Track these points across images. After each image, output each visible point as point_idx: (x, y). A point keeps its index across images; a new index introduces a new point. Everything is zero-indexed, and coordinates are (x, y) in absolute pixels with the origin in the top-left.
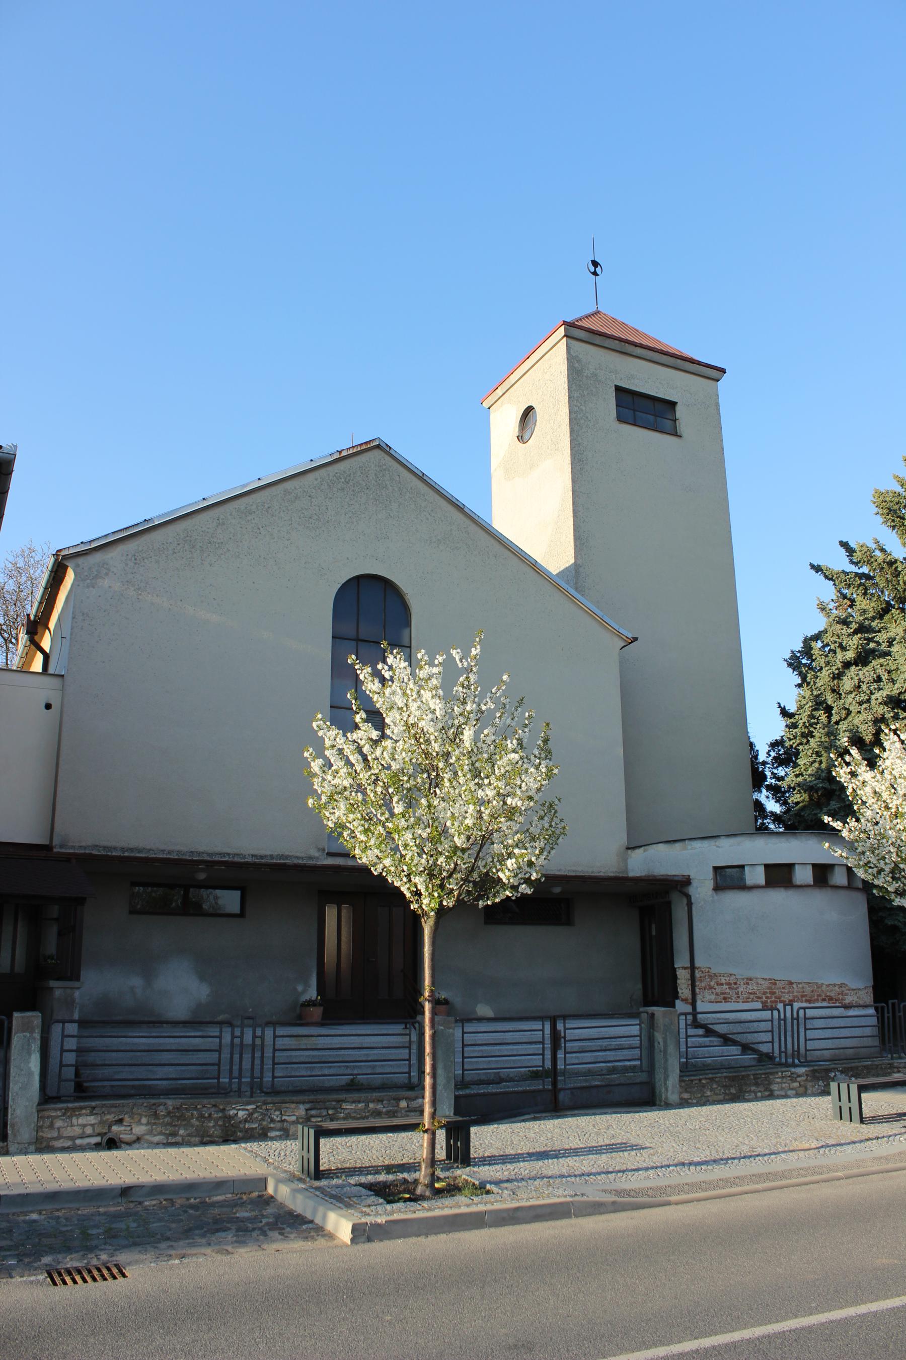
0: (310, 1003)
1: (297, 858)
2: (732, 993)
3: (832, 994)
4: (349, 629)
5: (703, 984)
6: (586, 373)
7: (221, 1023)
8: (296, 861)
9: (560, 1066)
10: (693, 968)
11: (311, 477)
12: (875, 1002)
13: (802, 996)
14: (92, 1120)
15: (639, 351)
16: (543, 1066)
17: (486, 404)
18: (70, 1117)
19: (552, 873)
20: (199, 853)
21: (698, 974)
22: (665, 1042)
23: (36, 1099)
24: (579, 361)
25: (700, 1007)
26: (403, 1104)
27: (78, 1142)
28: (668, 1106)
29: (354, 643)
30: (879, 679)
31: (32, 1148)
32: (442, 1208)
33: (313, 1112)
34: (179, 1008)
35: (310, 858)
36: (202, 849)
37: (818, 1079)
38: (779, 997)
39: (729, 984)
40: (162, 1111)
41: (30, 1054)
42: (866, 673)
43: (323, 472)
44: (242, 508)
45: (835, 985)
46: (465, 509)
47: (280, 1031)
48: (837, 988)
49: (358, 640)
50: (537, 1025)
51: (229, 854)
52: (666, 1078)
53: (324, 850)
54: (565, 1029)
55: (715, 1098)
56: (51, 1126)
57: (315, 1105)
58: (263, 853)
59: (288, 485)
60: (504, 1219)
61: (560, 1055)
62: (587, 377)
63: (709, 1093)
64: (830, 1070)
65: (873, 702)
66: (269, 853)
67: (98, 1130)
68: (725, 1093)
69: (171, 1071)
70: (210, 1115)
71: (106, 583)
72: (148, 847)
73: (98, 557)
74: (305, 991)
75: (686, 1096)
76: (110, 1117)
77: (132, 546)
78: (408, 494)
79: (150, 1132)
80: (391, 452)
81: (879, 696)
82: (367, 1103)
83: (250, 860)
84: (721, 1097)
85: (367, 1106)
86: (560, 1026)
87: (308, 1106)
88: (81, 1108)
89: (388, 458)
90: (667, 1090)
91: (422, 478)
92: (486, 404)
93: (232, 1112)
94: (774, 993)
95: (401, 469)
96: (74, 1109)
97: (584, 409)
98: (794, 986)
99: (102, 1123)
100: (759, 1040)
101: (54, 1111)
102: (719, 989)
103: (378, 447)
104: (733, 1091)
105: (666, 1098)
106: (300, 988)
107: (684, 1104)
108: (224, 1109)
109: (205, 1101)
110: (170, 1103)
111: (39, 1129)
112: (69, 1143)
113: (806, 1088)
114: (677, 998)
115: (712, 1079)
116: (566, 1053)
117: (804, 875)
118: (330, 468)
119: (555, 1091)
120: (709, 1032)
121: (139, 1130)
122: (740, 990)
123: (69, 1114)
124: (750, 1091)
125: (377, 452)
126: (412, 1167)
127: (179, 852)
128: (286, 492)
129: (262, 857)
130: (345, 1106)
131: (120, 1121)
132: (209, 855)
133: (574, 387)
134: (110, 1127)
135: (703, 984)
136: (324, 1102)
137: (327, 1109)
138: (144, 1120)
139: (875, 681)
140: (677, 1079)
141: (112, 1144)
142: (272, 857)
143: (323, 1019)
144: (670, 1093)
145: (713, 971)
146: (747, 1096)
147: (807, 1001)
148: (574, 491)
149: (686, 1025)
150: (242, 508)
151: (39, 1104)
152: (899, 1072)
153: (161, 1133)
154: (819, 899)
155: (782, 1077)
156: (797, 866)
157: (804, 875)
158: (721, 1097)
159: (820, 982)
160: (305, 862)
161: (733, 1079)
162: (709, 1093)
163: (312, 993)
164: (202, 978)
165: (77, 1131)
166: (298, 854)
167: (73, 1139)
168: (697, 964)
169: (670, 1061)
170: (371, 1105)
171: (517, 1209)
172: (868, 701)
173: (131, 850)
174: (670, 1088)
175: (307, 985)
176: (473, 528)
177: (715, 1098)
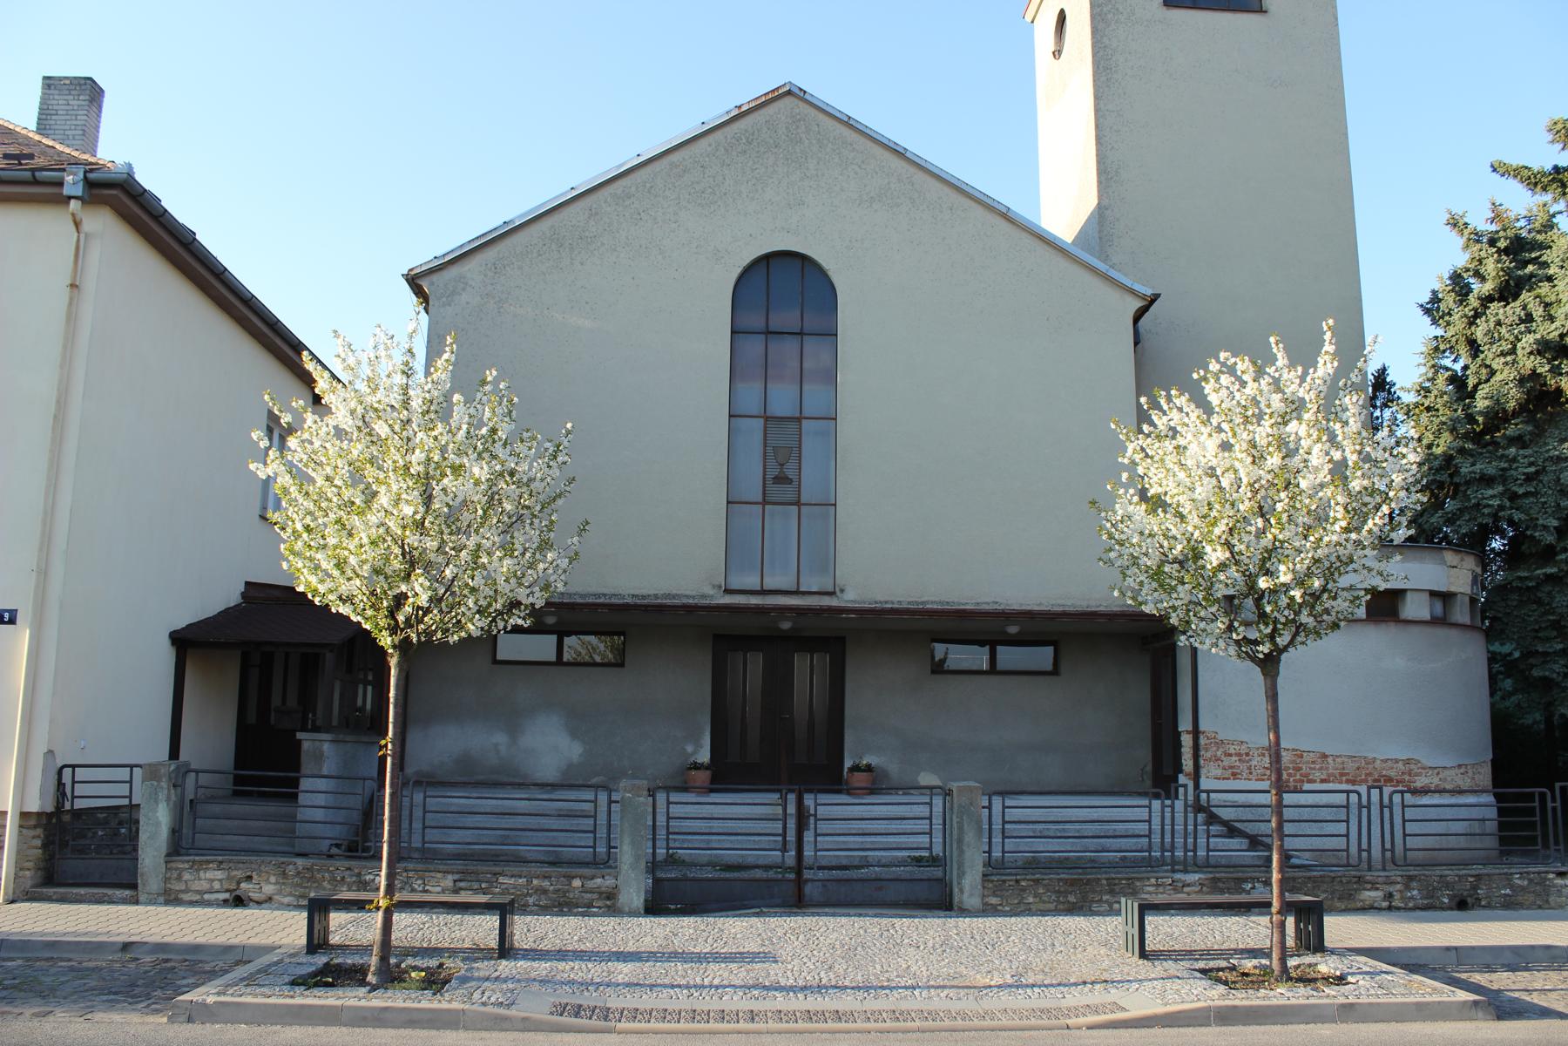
0: (696, 766)
1: (687, 597)
2: (1243, 766)
3: (1392, 774)
4: (757, 321)
5: (1208, 755)
7: (596, 787)
8: (685, 601)
9: (808, 852)
10: (1196, 733)
11: (704, 142)
12: (1495, 786)
13: (1342, 775)
14: (219, 874)
16: (930, 849)
17: (1028, 18)
18: (198, 870)
21: (1203, 741)
22: (961, 829)
23: (164, 850)
25: (1205, 784)
26: (577, 883)
27: (206, 896)
28: (964, 912)
29: (763, 337)
30: (1529, 318)
31: (161, 899)
32: (256, 996)
33: (462, 884)
34: (548, 767)
35: (704, 596)
38: (1306, 775)
39: (1239, 755)
40: (291, 870)
41: (156, 802)
42: (1513, 310)
43: (719, 135)
45: (1397, 761)
47: (674, 797)
48: (1400, 765)
49: (768, 332)
52: (961, 875)
54: (817, 805)
55: (1041, 906)
56: (179, 878)
57: (465, 875)
58: (644, 592)
59: (675, 157)
60: (365, 1019)
61: (808, 836)
63: (1031, 900)
64: (1245, 880)
65: (1519, 352)
66: (652, 592)
67: (226, 886)
68: (1058, 902)
69: (467, 835)
70: (343, 879)
71: (464, 297)
73: (454, 271)
74: (695, 753)
75: (994, 900)
76: (238, 874)
77: (491, 254)
79: (280, 892)
81: (1528, 341)
82: (530, 879)
83: (629, 600)
84: (1052, 906)
85: (530, 882)
86: (809, 800)
87: (456, 877)
88: (208, 862)
90: (961, 891)
91: (848, 123)
92: (1028, 18)
93: (368, 878)
94: (1299, 769)
95: (821, 116)
96: (201, 863)
98: (1330, 760)
99: (229, 878)
101: (181, 864)
102: (1227, 762)
103: (789, 93)
104: (1072, 899)
105: (961, 902)
106: (690, 749)
107: (987, 911)
108: (359, 875)
109: (338, 864)
110: (300, 862)
111: (167, 880)
112: (198, 897)
114: (1181, 771)
115: (1037, 881)
116: (816, 835)
118: (726, 129)
119: (800, 882)
120: (1212, 819)
121: (269, 889)
122: (1254, 763)
123: (197, 867)
124: (1100, 901)
125: (788, 100)
126: (365, 949)
129: (644, 597)
130: (501, 879)
131: (249, 878)
132: (582, 596)
134: (239, 883)
135: (1208, 755)
136: (476, 873)
137: (480, 882)
138: (273, 879)
139: (1522, 321)
140: (979, 878)
141: (239, 901)
142: (656, 596)
143: (712, 782)
144: (966, 895)
145: (1220, 737)
146: (1095, 907)
147: (1348, 781)
148: (1097, 111)
149: (1186, 806)
151: (168, 855)
153: (290, 894)
154: (1377, 640)
155: (1158, 885)
158: (1052, 906)
159: (1371, 755)
161: (1073, 883)
162: (1031, 900)
163: (704, 756)
164: (574, 734)
165: (205, 885)
167: (201, 893)
168: (1202, 728)
169: (968, 854)
170: (535, 882)
171: (386, 1009)
172: (1513, 351)
174: (967, 888)
175: (698, 746)
176: (920, 177)
177: (1041, 906)
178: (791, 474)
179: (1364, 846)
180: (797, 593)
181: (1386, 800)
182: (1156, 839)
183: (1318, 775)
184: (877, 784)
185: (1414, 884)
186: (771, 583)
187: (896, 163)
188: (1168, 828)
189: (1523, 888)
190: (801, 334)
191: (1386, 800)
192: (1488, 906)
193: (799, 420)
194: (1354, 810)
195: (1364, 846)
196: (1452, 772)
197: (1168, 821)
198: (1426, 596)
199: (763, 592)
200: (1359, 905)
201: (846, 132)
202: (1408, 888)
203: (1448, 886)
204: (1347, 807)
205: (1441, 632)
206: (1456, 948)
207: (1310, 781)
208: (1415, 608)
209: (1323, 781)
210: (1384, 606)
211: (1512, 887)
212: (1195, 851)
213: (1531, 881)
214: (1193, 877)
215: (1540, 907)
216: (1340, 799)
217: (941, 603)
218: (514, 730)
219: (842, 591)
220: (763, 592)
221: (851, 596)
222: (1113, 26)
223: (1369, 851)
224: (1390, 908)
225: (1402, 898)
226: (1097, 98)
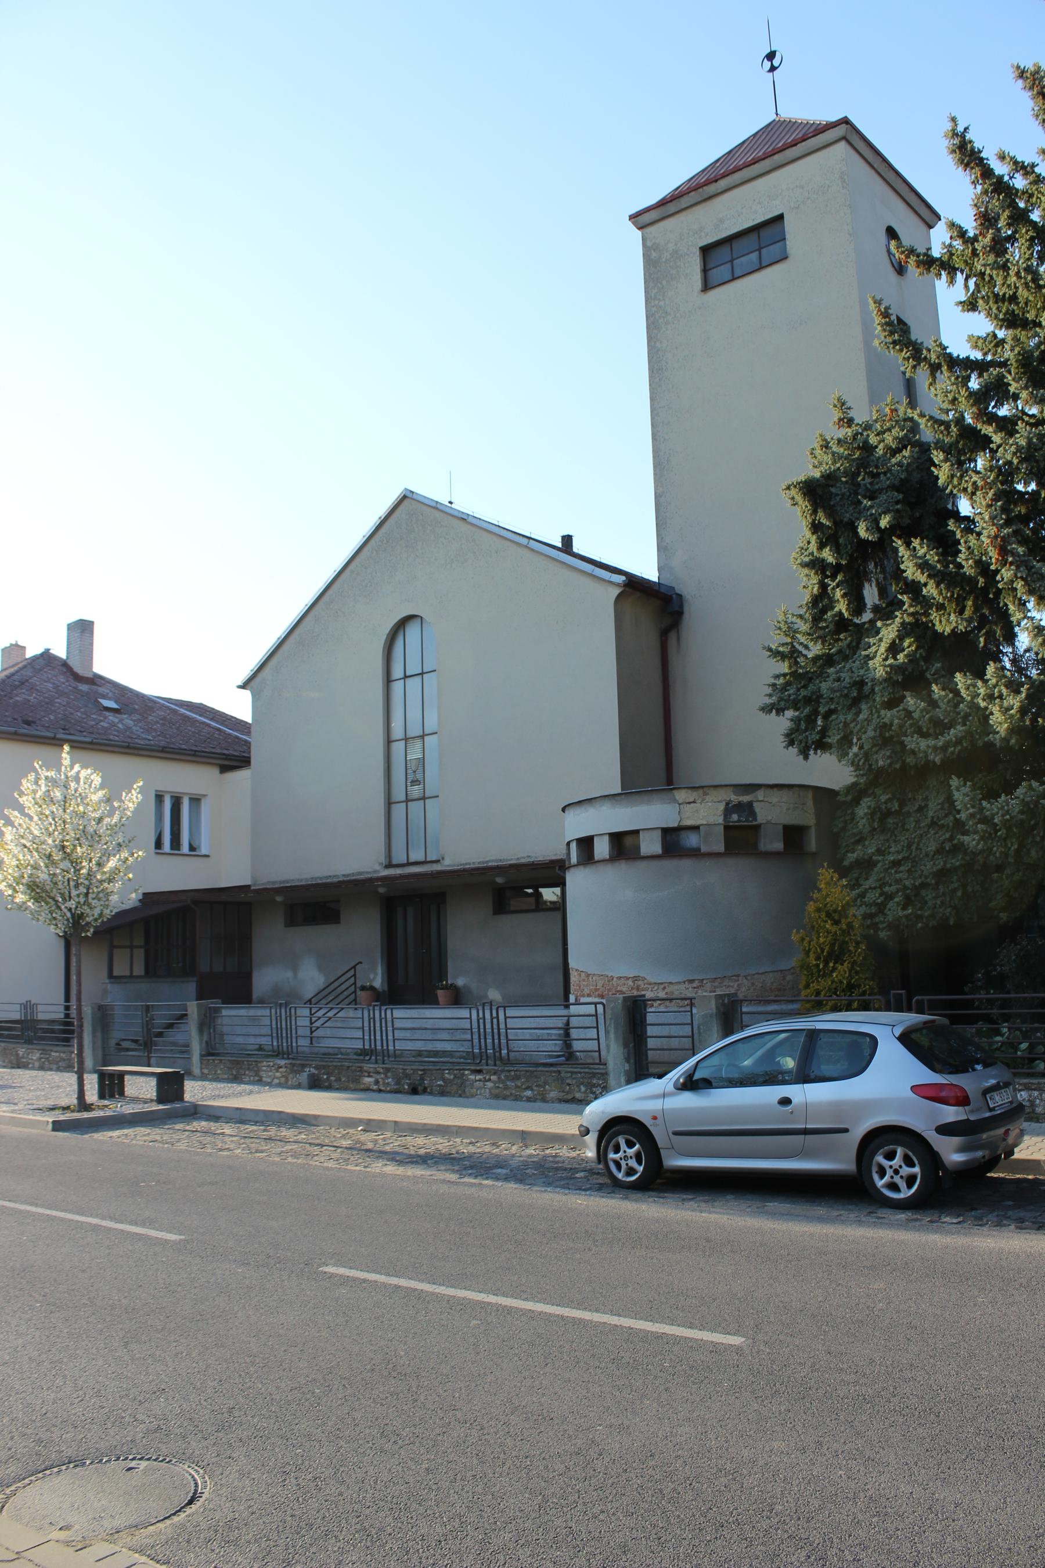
1: (368, 873)
6: (666, 255)
15: (723, 184)
20: (316, 878)
35: (375, 872)
36: (317, 875)
43: (372, 542)
45: (628, 978)
46: (470, 519)
48: (630, 982)
59: (352, 566)
62: (665, 262)
75: (206, 1071)
80: (415, 496)
97: (662, 303)
106: (372, 976)
113: (287, 1079)
117: (651, 845)
125: (406, 502)
127: (306, 879)
129: (348, 875)
132: (321, 878)
133: (651, 284)
152: (369, 1076)
156: (595, 839)
157: (602, 848)
159: (610, 974)
164: (321, 969)
173: (284, 882)
175: (376, 974)
178: (419, 776)
180: (425, 862)
183: (586, 991)
184: (458, 998)
185: (389, 1074)
186: (413, 858)
187: (464, 528)
188: (496, 1031)
189: (451, 1081)
190: (422, 674)
192: (431, 1093)
196: (682, 987)
197: (495, 1026)
200: (362, 1086)
201: (438, 514)
202: (387, 1077)
203: (407, 1076)
205: (670, 864)
206: (240, 1109)
207: (583, 996)
209: (589, 995)
210: (623, 845)
211: (443, 1079)
212: (486, 1049)
213: (455, 1075)
214: (282, 1062)
215: (460, 1096)
216: (591, 1009)
217: (496, 861)
218: (295, 969)
224: (380, 1091)
225: (384, 1083)
226: (652, 399)
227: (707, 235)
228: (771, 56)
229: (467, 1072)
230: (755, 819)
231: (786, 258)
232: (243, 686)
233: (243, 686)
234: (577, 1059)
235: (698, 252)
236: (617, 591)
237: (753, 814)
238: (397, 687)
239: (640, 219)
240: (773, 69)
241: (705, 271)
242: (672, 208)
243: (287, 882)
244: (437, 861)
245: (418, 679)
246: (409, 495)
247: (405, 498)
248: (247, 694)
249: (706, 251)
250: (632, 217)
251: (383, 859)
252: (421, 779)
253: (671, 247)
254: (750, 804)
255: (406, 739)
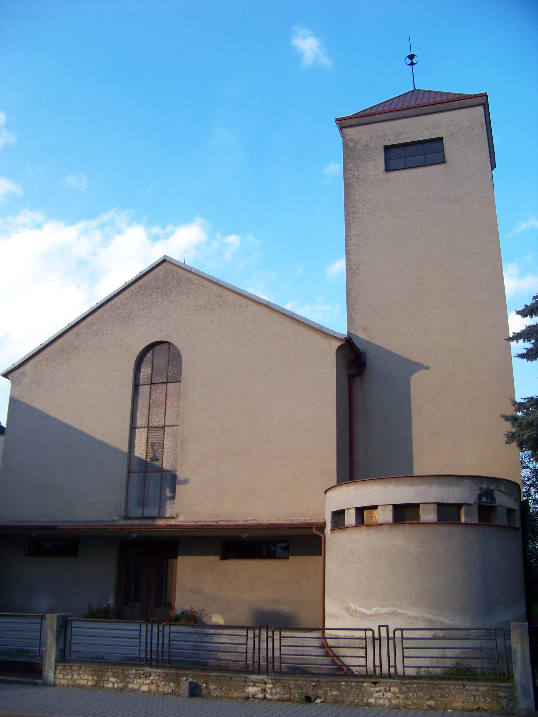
1: (107, 521)
6: (360, 146)
11: (126, 292)
19: (272, 522)
20: (57, 522)
24: (353, 140)
37: (170, 681)
43: (132, 288)
44: (88, 323)
50: (244, 632)
51: (71, 521)
53: (121, 516)
66: (92, 519)
72: (34, 520)
78: (183, 283)
89: (171, 266)
97: (356, 173)
100: (344, 654)
125: (164, 265)
128: (113, 306)
129: (88, 522)
150: (88, 323)
160: (110, 523)
166: (107, 519)
173: (26, 522)
179: (377, 664)
181: (391, 635)
182: (250, 655)
191: (391, 635)
193: (163, 427)
194: (369, 641)
195: (377, 664)
198: (436, 505)
199: (143, 518)
204: (365, 638)
205: (444, 529)
208: (428, 515)
217: (226, 521)
219: (177, 516)
220: (143, 518)
221: (182, 520)
222: (357, 189)
223: (381, 666)
227: (390, 139)
228: (411, 57)
229: (365, 684)
230: (495, 502)
231: (445, 162)
232: (6, 375)
233: (6, 375)
234: (352, 672)
235: (383, 149)
236: (338, 344)
237: (493, 498)
238: (144, 390)
239: (343, 124)
240: (412, 64)
241: (386, 160)
242: (365, 120)
243: (30, 522)
244: (172, 518)
245: (164, 386)
246: (166, 259)
247: (164, 261)
248: (7, 383)
249: (387, 148)
250: (339, 121)
251: (122, 512)
252: (160, 458)
253: (363, 142)
254: (492, 491)
255: (149, 428)
